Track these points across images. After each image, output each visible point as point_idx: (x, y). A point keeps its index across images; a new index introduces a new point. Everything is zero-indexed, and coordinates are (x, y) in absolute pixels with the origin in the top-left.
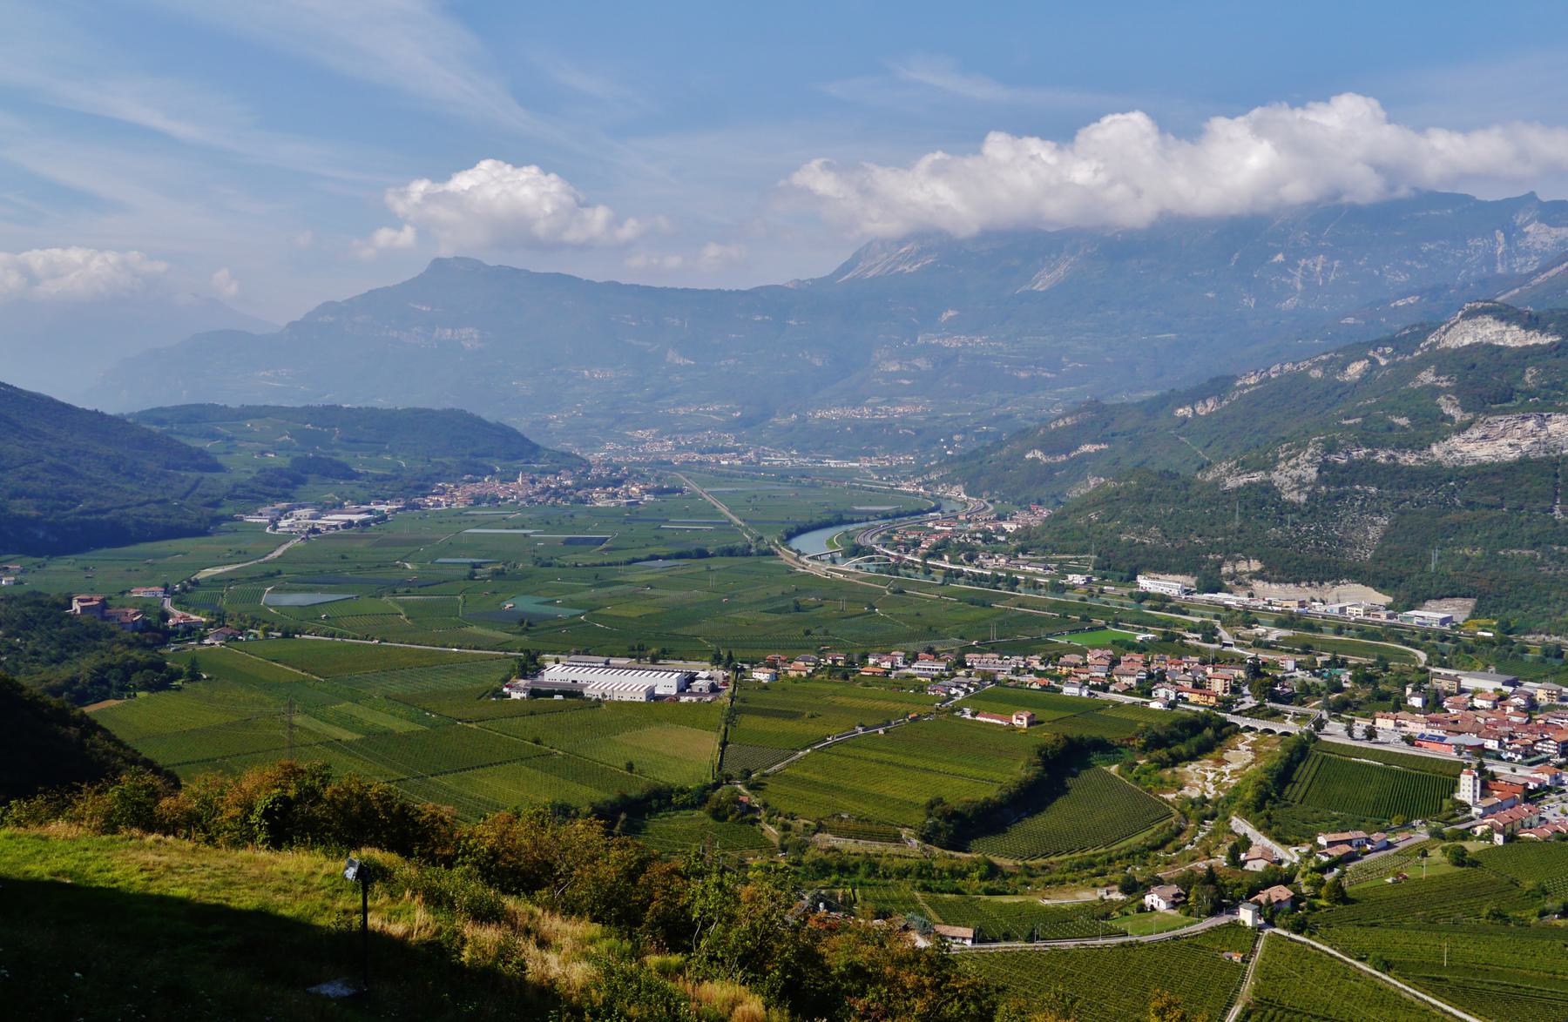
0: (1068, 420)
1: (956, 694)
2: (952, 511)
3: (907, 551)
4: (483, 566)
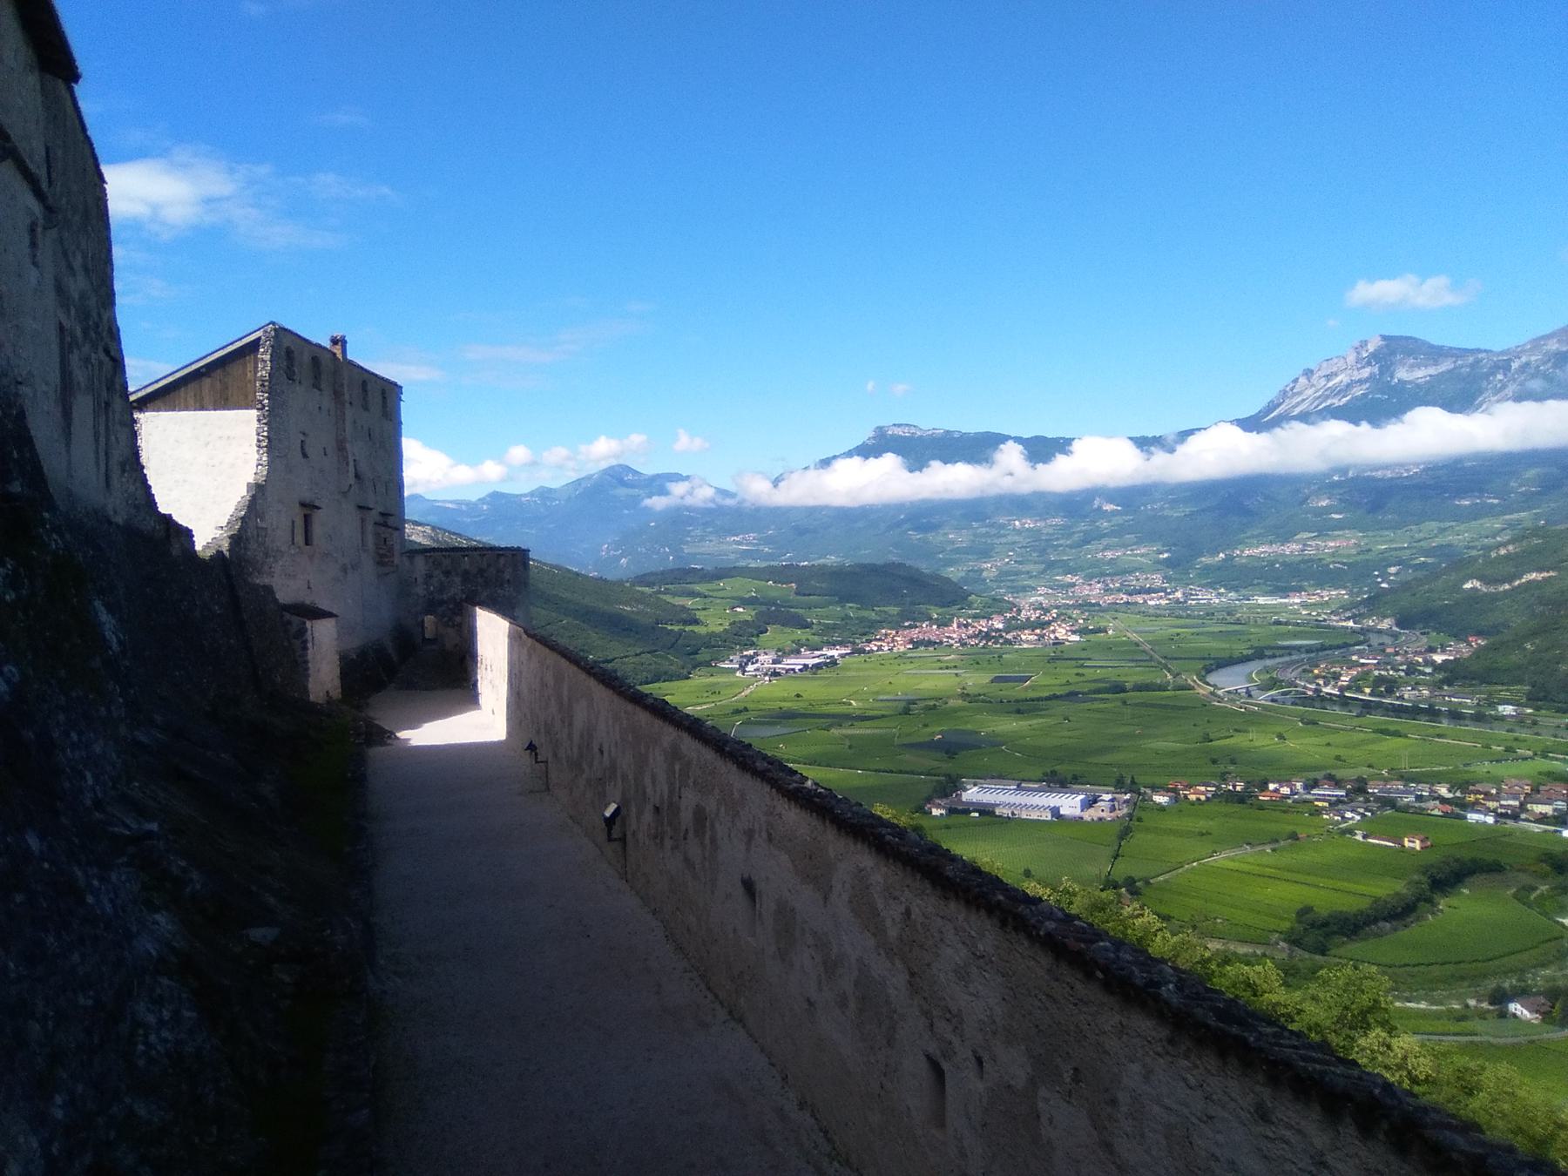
0: (1511, 548)
1: (1352, 818)
2: (1380, 644)
3: (1326, 685)
4: (918, 702)
